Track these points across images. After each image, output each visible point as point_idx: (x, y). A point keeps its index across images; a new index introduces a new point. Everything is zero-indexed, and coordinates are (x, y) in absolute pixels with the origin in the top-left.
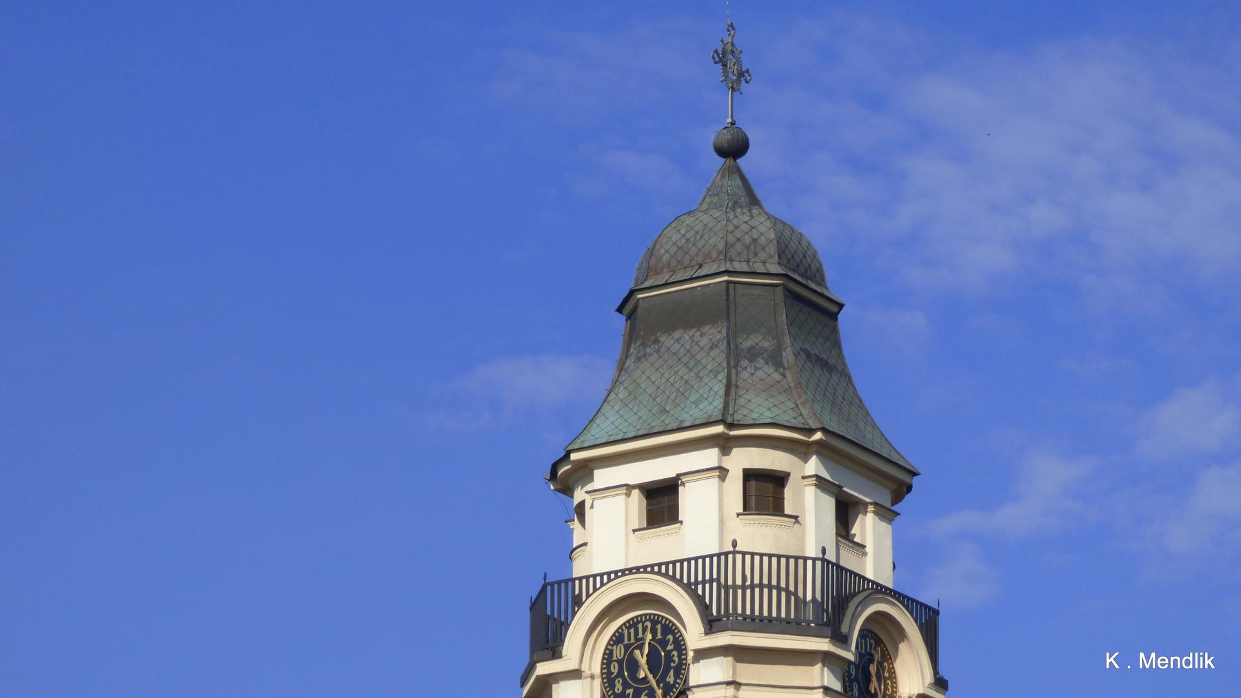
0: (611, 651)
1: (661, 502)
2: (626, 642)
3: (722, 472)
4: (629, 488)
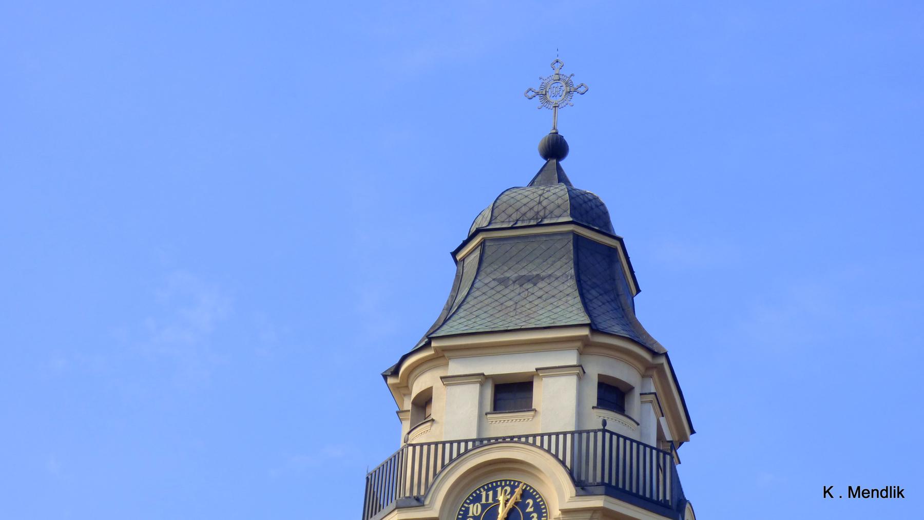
0: (467, 510)
1: (511, 393)
2: (484, 501)
3: (580, 371)
4: (483, 379)
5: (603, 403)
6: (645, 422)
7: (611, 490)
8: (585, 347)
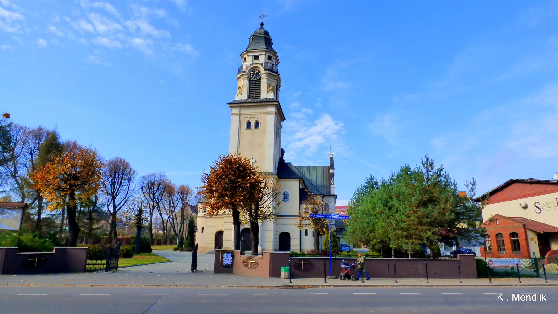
1: (256, 58)
4: (253, 56)
6: (274, 62)
7: (269, 70)
8: (266, 52)
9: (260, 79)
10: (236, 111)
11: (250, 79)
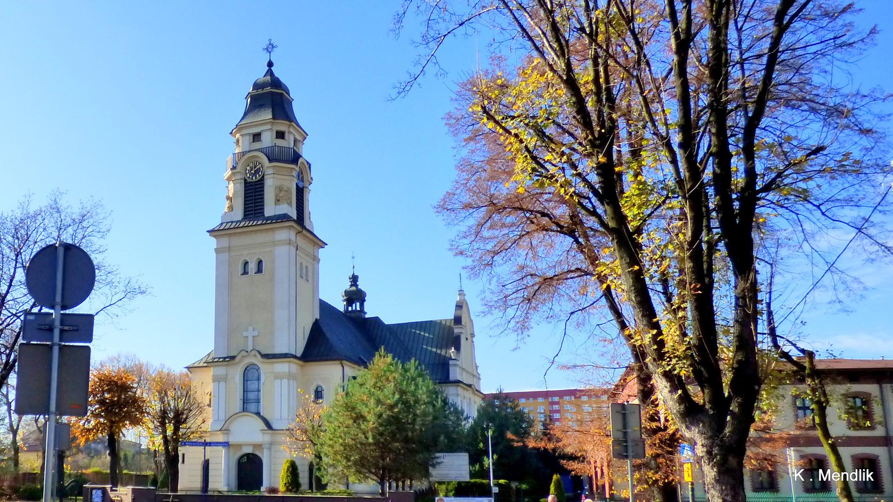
5: (277, 137)
8: (272, 124)
9: (261, 181)
10: (225, 242)
11: (245, 180)
